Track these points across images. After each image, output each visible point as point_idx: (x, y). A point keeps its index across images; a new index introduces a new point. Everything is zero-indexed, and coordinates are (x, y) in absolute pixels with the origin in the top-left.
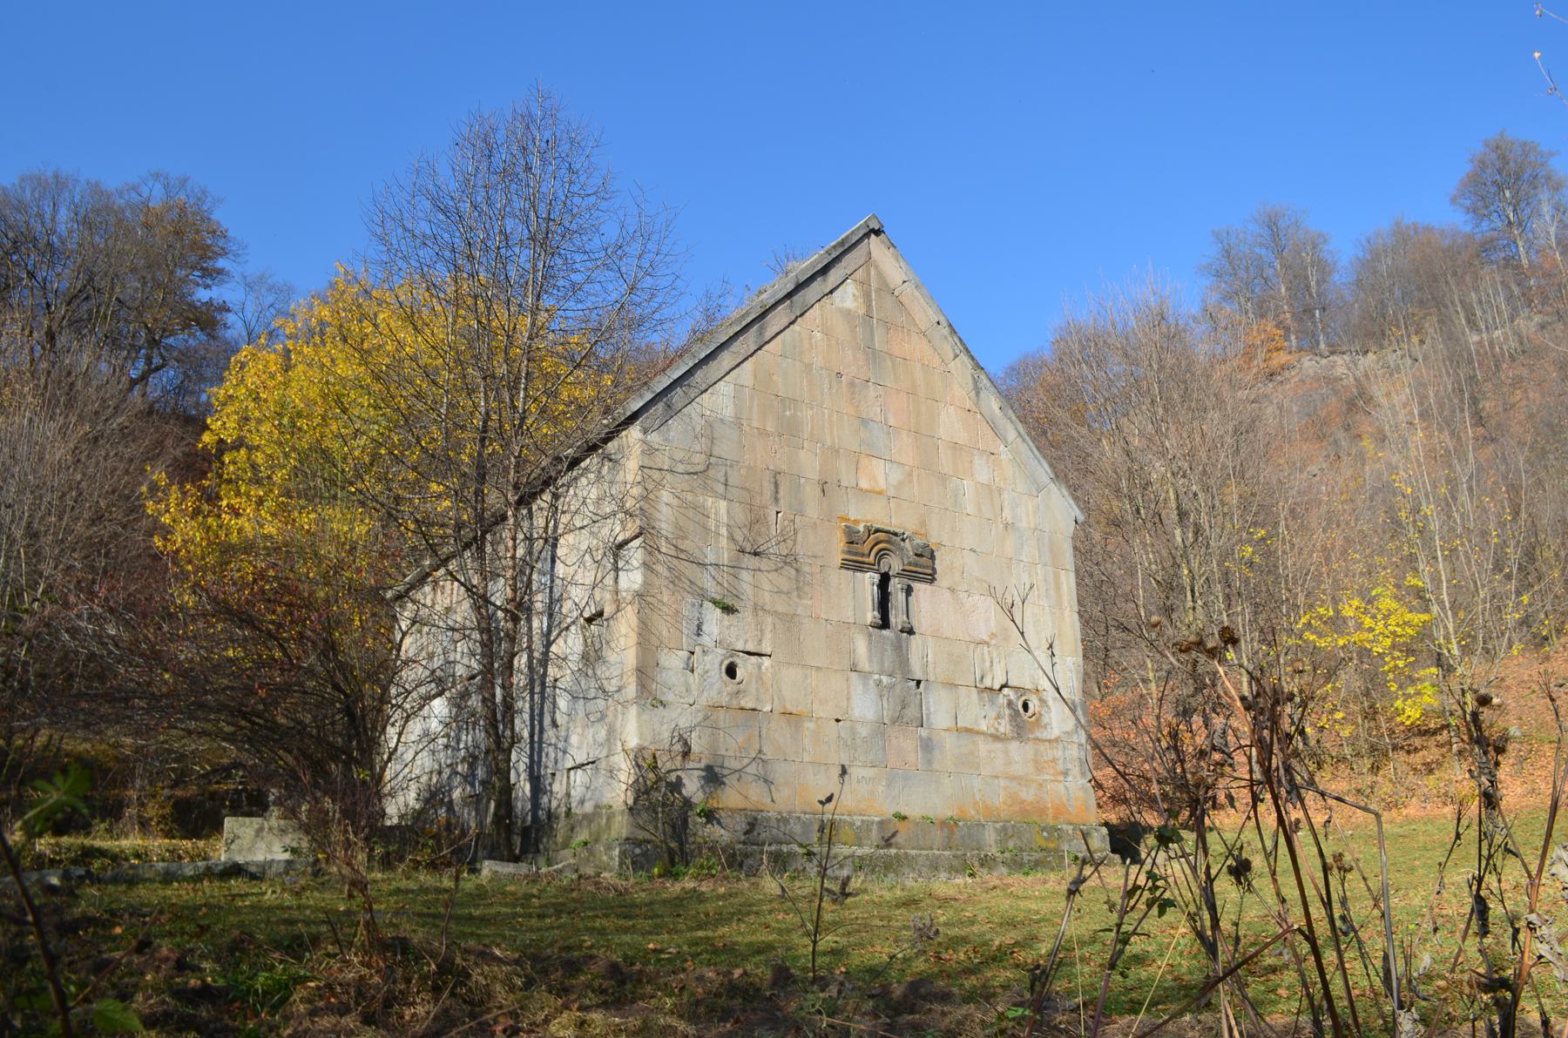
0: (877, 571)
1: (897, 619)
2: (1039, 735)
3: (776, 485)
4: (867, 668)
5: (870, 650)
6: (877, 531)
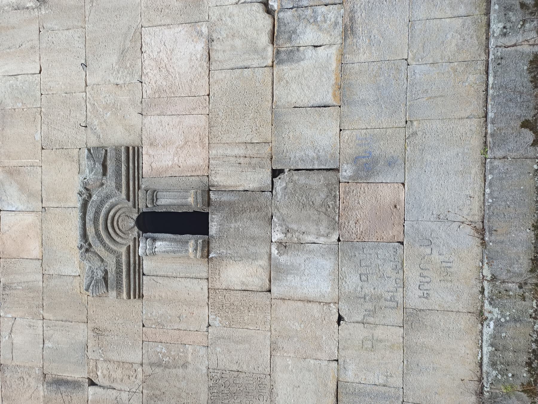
1: (191, 202)
4: (264, 262)
5: (241, 258)
6: (85, 236)
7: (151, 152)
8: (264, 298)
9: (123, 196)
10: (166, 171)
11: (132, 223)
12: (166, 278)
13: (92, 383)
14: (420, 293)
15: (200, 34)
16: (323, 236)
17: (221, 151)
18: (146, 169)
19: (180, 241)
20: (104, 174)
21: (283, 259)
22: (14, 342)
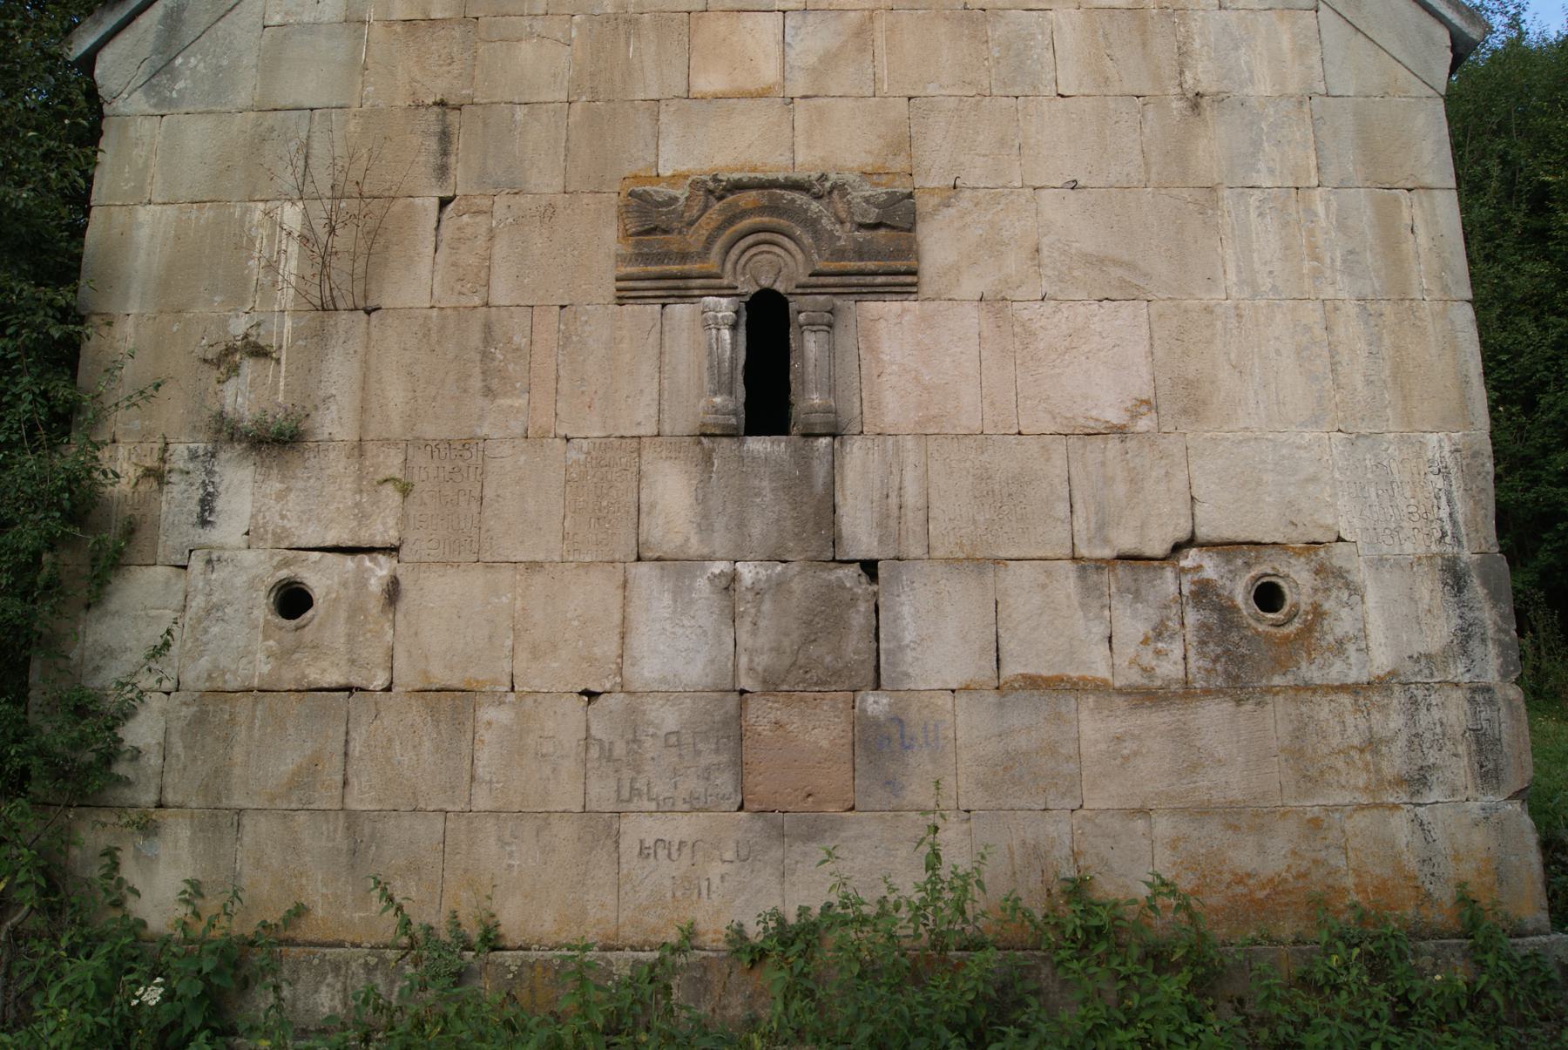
0: (729, 291)
1: (809, 399)
2: (1311, 672)
3: (445, 137)
4: (695, 547)
5: (702, 500)
6: (738, 187)
7: (907, 318)
8: (626, 549)
9: (821, 265)
10: (871, 349)
11: (765, 282)
12: (657, 351)
13: (444, 203)
14: (649, 842)
15: (1135, 416)
16: (751, 661)
17: (911, 458)
18: (873, 307)
19: (732, 379)
20: (861, 226)
21: (702, 583)
22: (523, 45)
